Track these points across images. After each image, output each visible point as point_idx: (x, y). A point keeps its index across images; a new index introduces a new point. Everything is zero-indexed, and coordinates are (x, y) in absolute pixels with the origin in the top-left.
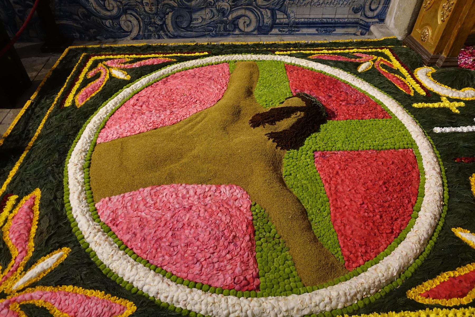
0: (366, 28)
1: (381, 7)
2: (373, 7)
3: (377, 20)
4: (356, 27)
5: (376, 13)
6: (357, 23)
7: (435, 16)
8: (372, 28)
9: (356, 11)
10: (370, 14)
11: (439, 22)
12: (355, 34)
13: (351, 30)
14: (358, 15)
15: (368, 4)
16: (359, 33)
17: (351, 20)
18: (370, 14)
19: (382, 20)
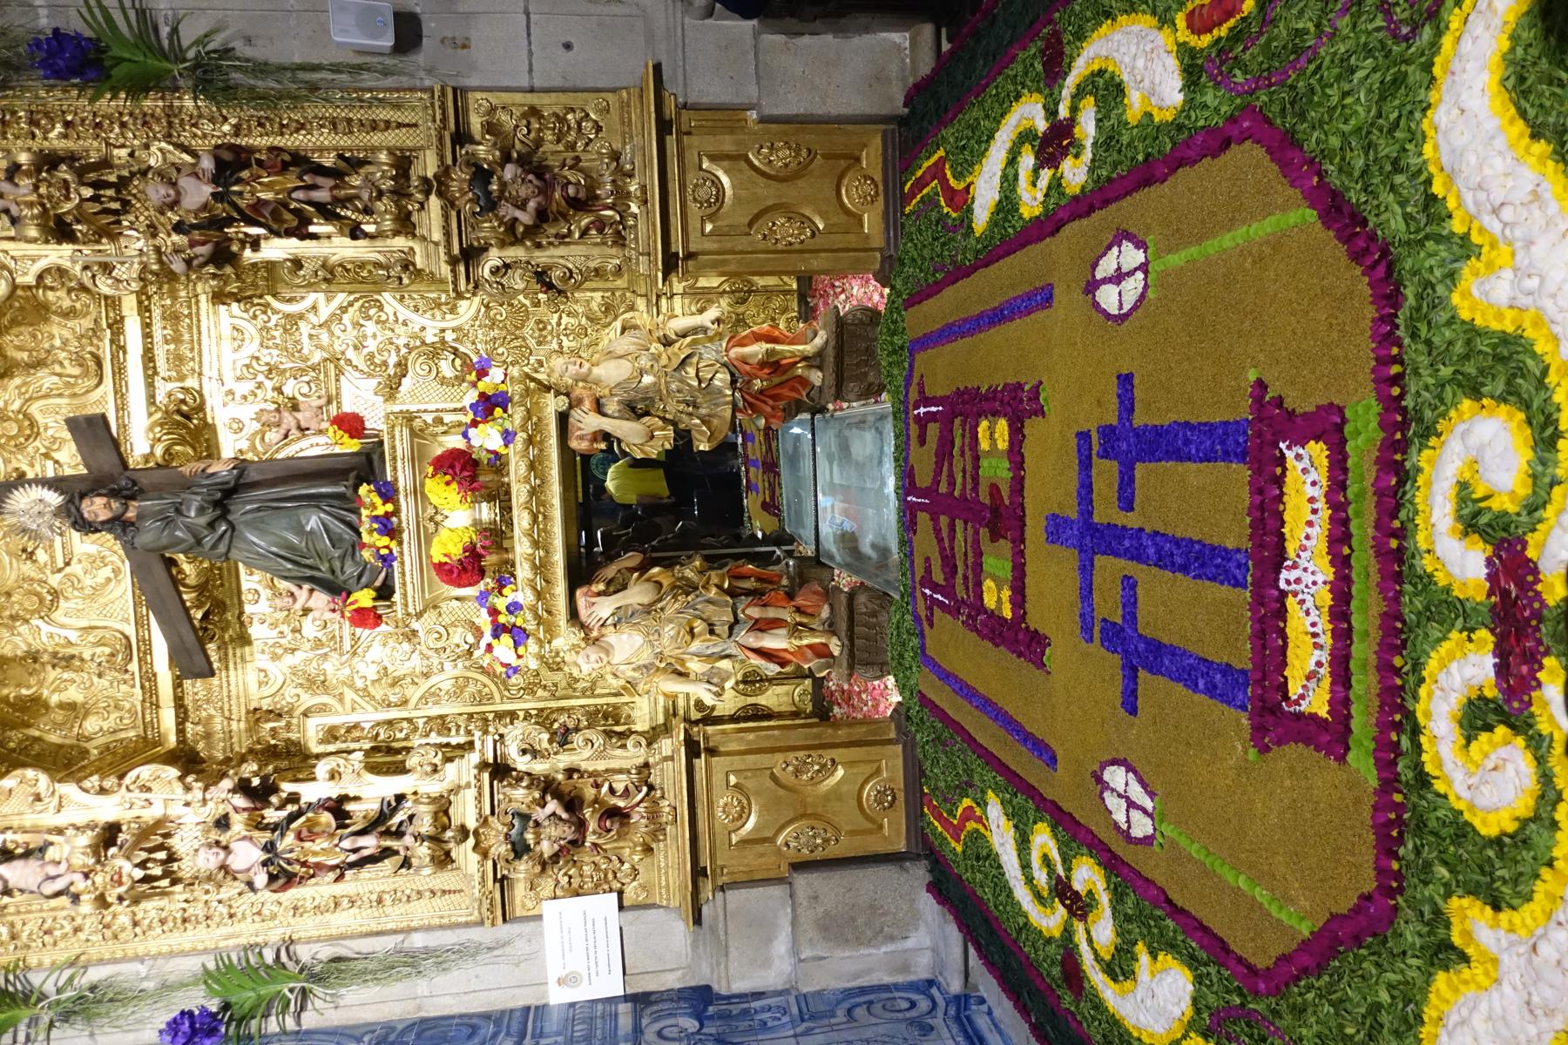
0: (962, 1002)
1: (897, 994)
2: (905, 1005)
3: (934, 991)
4: (968, 1018)
5: (914, 997)
6: (958, 1019)
7: (836, 794)
8: (955, 986)
9: (927, 1030)
10: (924, 1005)
11: (840, 772)
12: (990, 1013)
13: (982, 1023)
14: (938, 1021)
15: (900, 1015)
16: (984, 1008)
17: (955, 1029)
18: (924, 1005)
19: (931, 983)
